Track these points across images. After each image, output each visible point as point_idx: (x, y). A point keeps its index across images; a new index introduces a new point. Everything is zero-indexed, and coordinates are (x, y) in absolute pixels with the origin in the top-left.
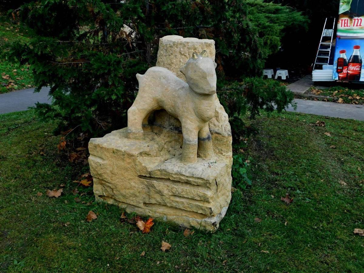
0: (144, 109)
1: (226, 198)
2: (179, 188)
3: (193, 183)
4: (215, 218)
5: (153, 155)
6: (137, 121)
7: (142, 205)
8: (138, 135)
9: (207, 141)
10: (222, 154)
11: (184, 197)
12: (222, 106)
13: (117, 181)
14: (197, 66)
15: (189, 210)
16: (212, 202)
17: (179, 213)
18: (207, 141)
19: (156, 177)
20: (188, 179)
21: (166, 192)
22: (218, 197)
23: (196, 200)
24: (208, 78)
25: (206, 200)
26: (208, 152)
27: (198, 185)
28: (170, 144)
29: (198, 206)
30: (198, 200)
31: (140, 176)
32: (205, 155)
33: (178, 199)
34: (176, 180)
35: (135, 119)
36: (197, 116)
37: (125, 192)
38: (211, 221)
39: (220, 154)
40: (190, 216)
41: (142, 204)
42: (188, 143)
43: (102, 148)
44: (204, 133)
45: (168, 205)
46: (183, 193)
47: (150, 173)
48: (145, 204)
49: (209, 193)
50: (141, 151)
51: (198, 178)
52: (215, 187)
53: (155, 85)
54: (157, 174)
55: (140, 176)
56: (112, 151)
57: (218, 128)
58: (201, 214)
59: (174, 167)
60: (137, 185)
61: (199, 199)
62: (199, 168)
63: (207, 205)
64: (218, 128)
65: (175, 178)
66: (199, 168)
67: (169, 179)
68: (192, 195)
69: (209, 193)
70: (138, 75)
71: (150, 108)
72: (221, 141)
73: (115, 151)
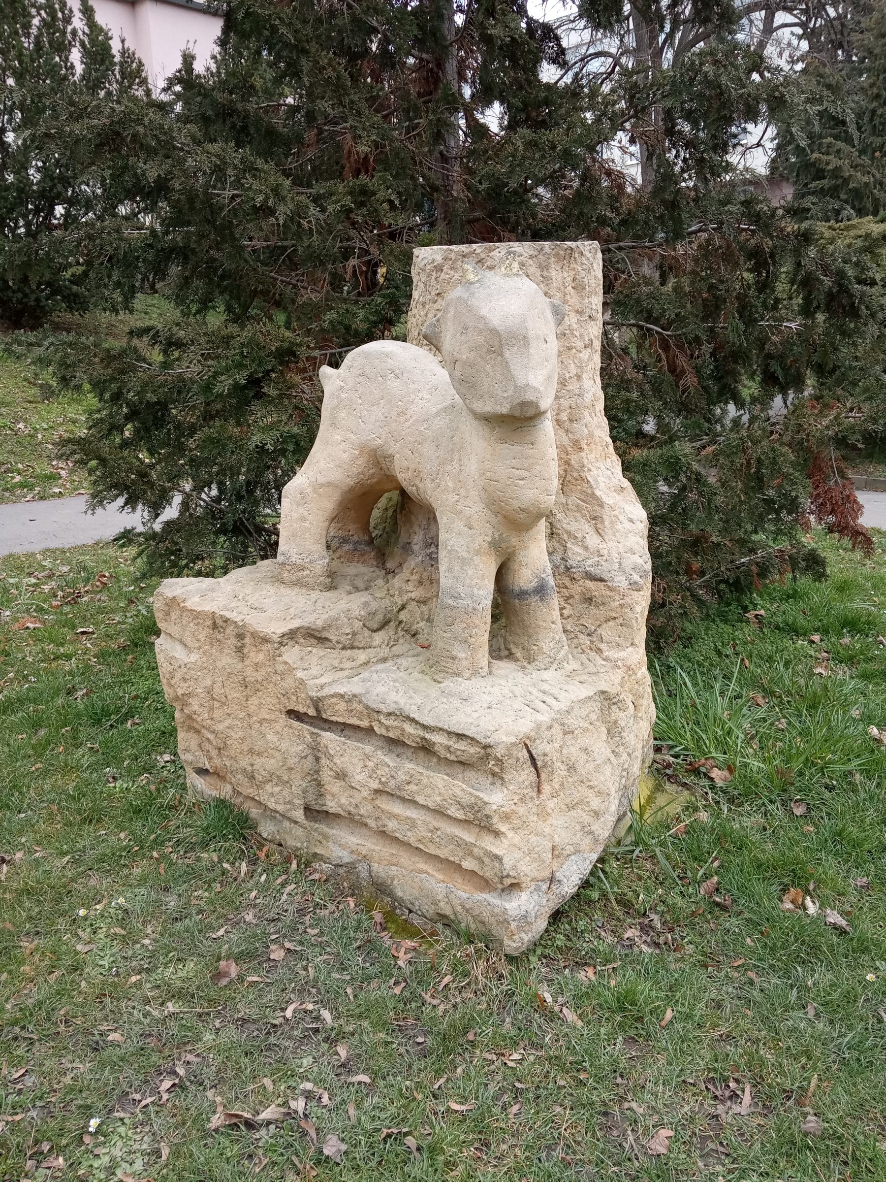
0: (329, 484)
1: (587, 819)
2: (407, 768)
3: (443, 753)
4: (524, 896)
5: (338, 642)
6: (307, 524)
7: (299, 815)
8: (307, 572)
9: (534, 599)
10: (599, 651)
11: (412, 802)
12: (626, 483)
13: (227, 723)
14: (470, 309)
15: (432, 850)
16: (510, 834)
17: (406, 859)
18: (534, 599)
19: (334, 719)
20: (427, 736)
21: (359, 777)
22: (543, 814)
23: (449, 817)
24: (507, 354)
25: (481, 821)
26: (537, 640)
27: (461, 763)
28: (424, 608)
29: (459, 843)
30: (456, 819)
31: (292, 714)
32: (528, 650)
33: (397, 808)
34: (391, 735)
35: (303, 519)
36: (488, 506)
37: (252, 765)
38: (507, 905)
39: (592, 654)
40: (441, 877)
41: (302, 812)
42: (450, 602)
43: (184, 609)
44: (524, 570)
45: (372, 823)
46: (412, 787)
47: (317, 703)
48: (307, 809)
49: (496, 798)
50: (295, 624)
51: (460, 736)
52: (527, 775)
53: (378, 399)
54: (337, 708)
55: (292, 714)
56: (209, 623)
57: (597, 559)
58: (473, 872)
59: (391, 685)
60: (288, 742)
61: (460, 815)
62: (494, 703)
63: (488, 844)
64: (597, 559)
65: (387, 728)
66: (494, 703)
67: (370, 731)
68: (438, 799)
69: (496, 798)
70: (326, 370)
71: (351, 482)
72: (603, 604)
73: (219, 622)
